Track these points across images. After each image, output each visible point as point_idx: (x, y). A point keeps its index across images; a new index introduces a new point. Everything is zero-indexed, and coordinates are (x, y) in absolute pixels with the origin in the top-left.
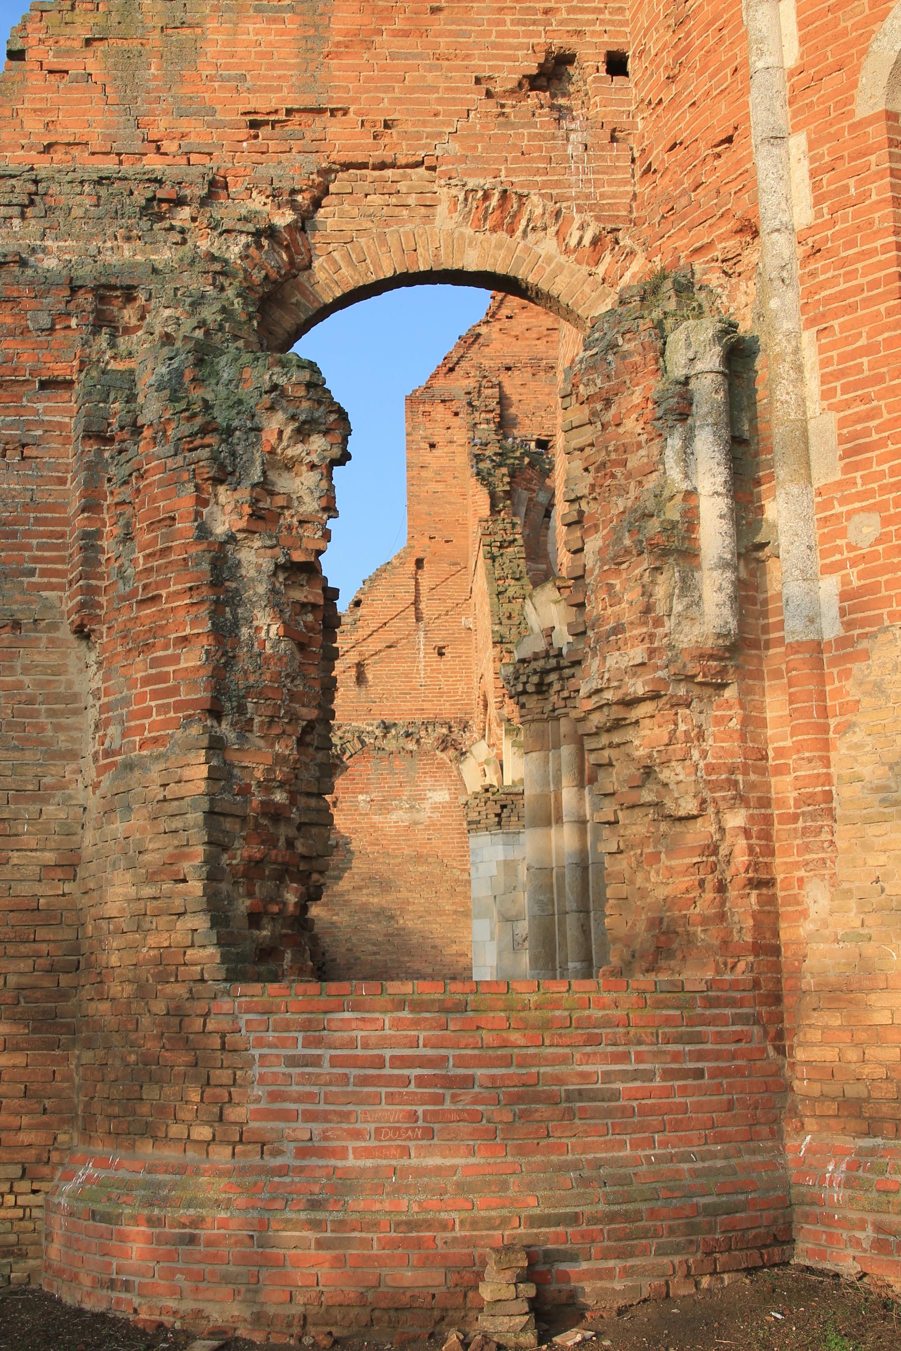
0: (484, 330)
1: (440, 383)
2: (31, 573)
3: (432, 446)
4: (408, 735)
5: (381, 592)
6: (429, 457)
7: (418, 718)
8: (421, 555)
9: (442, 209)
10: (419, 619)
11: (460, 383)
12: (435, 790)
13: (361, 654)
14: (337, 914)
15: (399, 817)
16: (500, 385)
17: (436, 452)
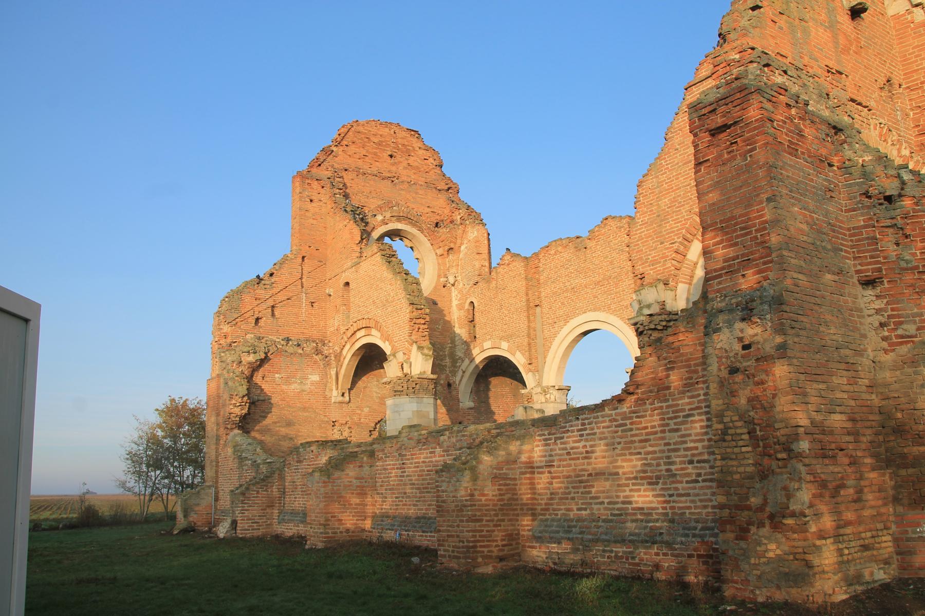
0: (334, 149)
1: (314, 170)
2: (841, 250)
4: (299, 345)
6: (309, 206)
7: (302, 337)
9: (872, 127)
10: (302, 287)
11: (324, 173)
13: (274, 301)
17: (313, 204)
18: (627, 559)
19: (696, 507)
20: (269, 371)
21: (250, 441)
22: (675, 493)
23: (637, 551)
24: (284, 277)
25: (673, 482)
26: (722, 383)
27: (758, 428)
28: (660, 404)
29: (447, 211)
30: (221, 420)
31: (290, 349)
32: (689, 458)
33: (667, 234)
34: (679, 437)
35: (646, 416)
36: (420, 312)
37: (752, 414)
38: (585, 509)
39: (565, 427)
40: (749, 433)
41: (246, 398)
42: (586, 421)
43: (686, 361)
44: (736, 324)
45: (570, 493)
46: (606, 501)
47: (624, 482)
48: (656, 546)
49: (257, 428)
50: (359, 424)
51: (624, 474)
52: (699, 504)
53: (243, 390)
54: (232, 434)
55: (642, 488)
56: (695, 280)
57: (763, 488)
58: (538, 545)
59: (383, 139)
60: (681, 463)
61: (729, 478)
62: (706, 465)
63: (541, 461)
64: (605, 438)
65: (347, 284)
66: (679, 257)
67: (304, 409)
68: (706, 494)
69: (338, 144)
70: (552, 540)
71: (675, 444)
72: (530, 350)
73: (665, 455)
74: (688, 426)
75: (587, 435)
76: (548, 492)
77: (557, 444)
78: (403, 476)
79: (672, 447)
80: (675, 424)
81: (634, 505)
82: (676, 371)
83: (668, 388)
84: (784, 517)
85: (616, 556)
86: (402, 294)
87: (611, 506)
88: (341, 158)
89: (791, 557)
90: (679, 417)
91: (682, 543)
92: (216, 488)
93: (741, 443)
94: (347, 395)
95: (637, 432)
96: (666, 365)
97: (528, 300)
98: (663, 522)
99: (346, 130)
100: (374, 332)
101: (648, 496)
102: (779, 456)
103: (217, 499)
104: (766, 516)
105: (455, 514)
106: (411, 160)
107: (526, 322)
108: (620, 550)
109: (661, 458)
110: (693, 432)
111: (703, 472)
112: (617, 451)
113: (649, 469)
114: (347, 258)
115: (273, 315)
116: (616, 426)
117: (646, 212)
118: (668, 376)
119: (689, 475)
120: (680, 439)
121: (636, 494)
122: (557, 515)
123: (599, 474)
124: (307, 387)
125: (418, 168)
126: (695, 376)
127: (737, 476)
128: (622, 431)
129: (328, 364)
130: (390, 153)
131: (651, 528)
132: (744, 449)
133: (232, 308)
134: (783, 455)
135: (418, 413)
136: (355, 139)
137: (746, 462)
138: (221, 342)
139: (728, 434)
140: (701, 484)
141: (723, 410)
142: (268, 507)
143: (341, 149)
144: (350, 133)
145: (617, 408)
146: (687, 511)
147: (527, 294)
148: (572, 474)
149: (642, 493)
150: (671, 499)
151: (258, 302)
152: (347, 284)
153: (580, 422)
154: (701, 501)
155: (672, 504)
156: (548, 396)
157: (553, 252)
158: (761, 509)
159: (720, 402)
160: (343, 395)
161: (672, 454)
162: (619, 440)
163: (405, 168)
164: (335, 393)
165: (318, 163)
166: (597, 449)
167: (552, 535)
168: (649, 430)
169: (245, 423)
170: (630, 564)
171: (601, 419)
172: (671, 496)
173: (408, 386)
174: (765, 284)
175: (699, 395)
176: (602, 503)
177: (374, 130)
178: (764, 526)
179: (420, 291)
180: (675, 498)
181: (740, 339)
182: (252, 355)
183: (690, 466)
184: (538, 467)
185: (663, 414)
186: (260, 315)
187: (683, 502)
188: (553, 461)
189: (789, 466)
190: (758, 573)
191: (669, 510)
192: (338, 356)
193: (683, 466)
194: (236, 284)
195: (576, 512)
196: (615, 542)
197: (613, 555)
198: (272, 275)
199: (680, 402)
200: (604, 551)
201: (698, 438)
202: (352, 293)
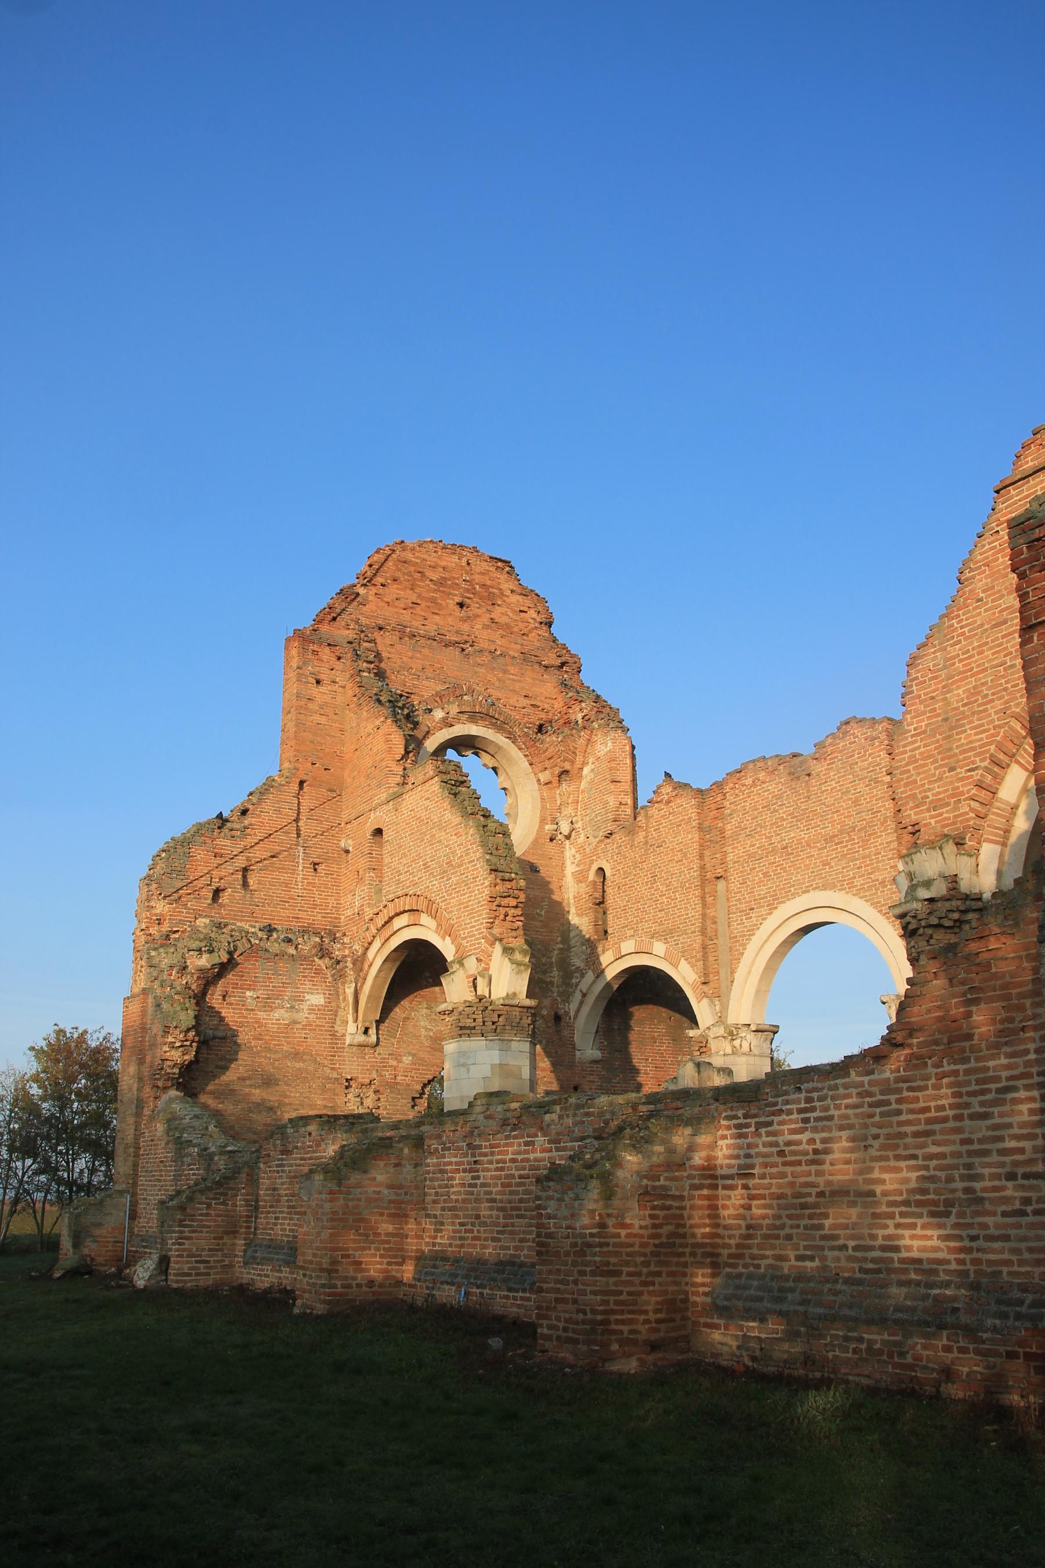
0: (362, 591)
1: (325, 628)
3: (318, 682)
4: (290, 941)
5: (268, 805)
6: (314, 691)
7: (295, 925)
8: (305, 778)
10: (299, 835)
11: (342, 633)
12: (312, 994)
13: (248, 859)
14: (223, 1103)
15: (281, 1014)
16: (373, 641)
17: (322, 689)
18: (891, 1355)
19: (1021, 1263)
20: (235, 986)
21: (197, 1110)
22: (982, 1233)
23: (910, 1342)
24: (268, 817)
25: (977, 1213)
28: (953, 1067)
29: (558, 705)
30: (146, 1071)
31: (274, 947)
32: (1008, 1169)
33: (962, 752)
34: (988, 1128)
35: (926, 1088)
36: (508, 885)
38: (812, 1258)
39: (776, 1104)
41: (192, 1034)
42: (815, 1095)
43: (1003, 987)
45: (782, 1227)
46: (851, 1243)
47: (884, 1209)
48: (945, 1333)
49: (210, 1088)
50: (393, 1085)
51: (885, 1194)
52: (1026, 1256)
53: (187, 1018)
54: (165, 1097)
56: (1013, 838)
58: (722, 1322)
59: (447, 575)
63: (729, 1166)
64: (850, 1127)
65: (379, 832)
66: (983, 795)
67: (297, 1056)
69: (368, 581)
70: (749, 1314)
71: (980, 1141)
72: (705, 958)
73: (961, 1161)
74: (1006, 1108)
75: (816, 1119)
76: (743, 1223)
77: (759, 1135)
78: (475, 1185)
79: (976, 1146)
80: (982, 1104)
81: (904, 1254)
82: (983, 1006)
83: (969, 1037)
85: (869, 1349)
86: (477, 853)
87: (859, 1254)
88: (373, 607)
90: (989, 1091)
91: (995, 1329)
92: (134, 1195)
94: (372, 1031)
95: (911, 1117)
96: (964, 994)
97: (702, 868)
98: (958, 1287)
99: (382, 557)
100: (425, 919)
101: (930, 1238)
103: (133, 1216)
105: (570, 1260)
106: (497, 613)
107: (699, 908)
108: (878, 1337)
110: (1016, 1119)
113: (932, 1186)
114: (379, 786)
115: (245, 884)
116: (870, 1105)
117: (924, 713)
118: (968, 1015)
119: (1006, 1200)
120: (991, 1133)
121: (907, 1233)
122: (758, 1266)
123: (839, 1194)
124: (301, 1016)
125: (507, 627)
126: (1019, 1016)
128: (882, 1114)
129: (340, 976)
130: (458, 599)
131: (935, 1296)
133: (171, 868)
135: (502, 1069)
136: (398, 574)
138: (152, 931)
140: (1030, 1219)
142: (228, 1233)
143: (373, 590)
144: (390, 563)
145: (872, 1072)
146: (1005, 1270)
147: (701, 857)
148: (788, 1191)
149: (918, 1231)
150: (973, 1244)
151: (219, 861)
152: (379, 832)
153: (803, 1096)
154: (1031, 1250)
155: (975, 1255)
156: (737, 1043)
157: (749, 781)
160: (366, 1031)
161: (977, 1160)
162: (875, 1131)
163: (485, 627)
164: (351, 1028)
165: (331, 615)
166: (836, 1146)
167: (749, 1304)
168: (933, 1114)
169: (190, 1079)
170: (896, 1366)
171: (841, 1091)
172: (973, 1238)
173: (484, 1019)
175: (1027, 1052)
176: (844, 1247)
177: (432, 559)
179: (509, 847)
180: (981, 1243)
182: (205, 956)
185: (958, 1084)
186: (222, 884)
187: (997, 1253)
188: (752, 1166)
191: (969, 1266)
192: (360, 962)
193: (997, 1183)
194: (180, 827)
195: (793, 1262)
196: (870, 1322)
197: (864, 1346)
198: (244, 812)
199: (991, 1064)
200: (847, 1339)
201: (1024, 1131)
202: (387, 848)
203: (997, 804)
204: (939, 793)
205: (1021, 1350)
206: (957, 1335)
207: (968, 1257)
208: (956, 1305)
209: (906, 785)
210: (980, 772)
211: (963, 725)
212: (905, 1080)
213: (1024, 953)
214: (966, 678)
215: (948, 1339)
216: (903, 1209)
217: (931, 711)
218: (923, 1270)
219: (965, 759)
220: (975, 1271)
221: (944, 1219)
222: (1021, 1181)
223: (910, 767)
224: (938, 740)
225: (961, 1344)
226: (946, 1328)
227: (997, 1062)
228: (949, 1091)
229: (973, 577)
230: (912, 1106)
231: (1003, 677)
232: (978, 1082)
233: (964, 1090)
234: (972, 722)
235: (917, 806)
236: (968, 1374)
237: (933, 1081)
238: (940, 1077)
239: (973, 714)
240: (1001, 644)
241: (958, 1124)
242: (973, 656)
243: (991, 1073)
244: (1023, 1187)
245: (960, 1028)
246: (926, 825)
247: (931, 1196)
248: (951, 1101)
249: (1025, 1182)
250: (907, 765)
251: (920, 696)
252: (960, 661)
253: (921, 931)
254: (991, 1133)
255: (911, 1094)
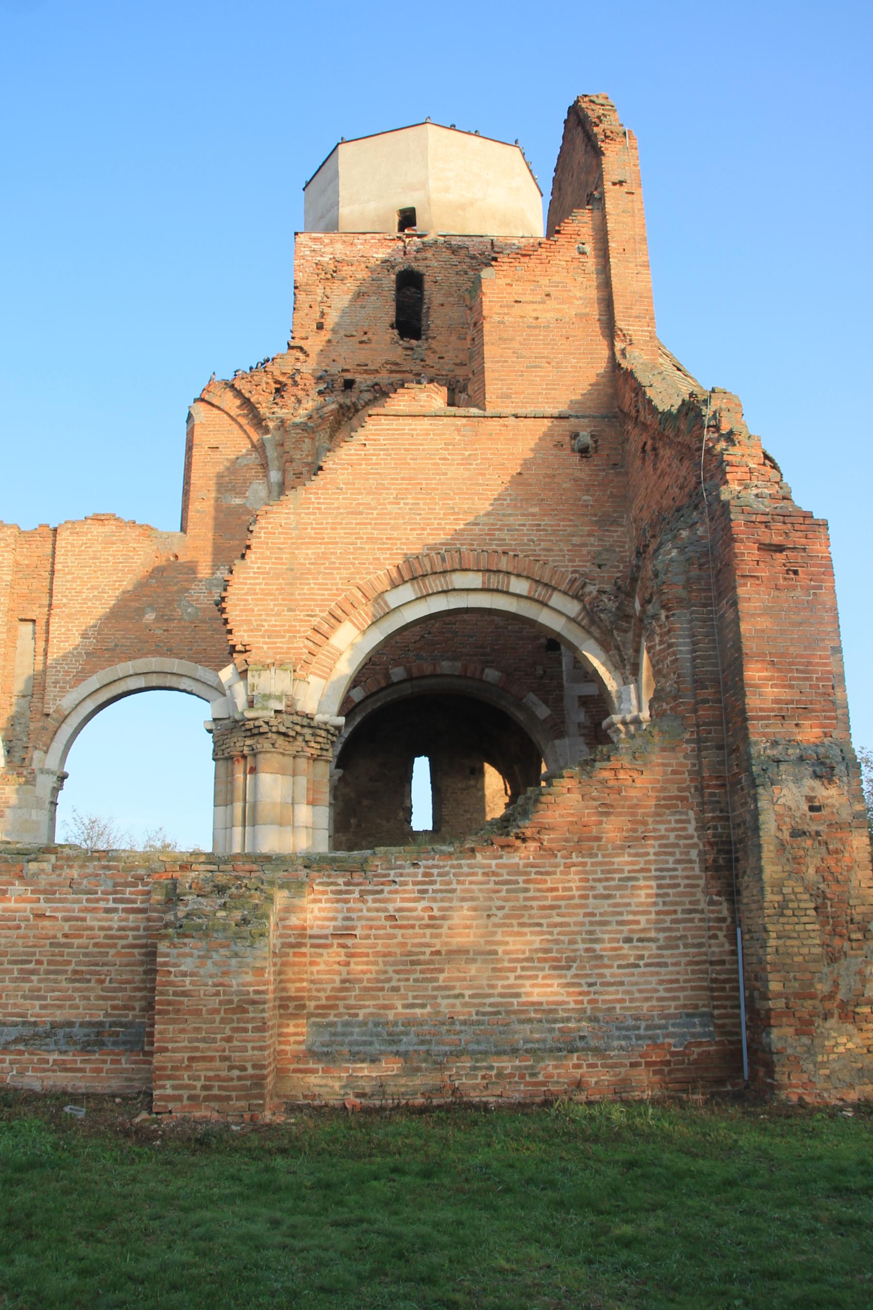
18: (522, 1077)
19: (632, 1000)
22: (599, 981)
23: (542, 1064)
25: (597, 967)
26: (782, 846)
27: (829, 903)
28: (580, 859)
32: (625, 935)
33: (302, 600)
34: (609, 905)
35: (554, 873)
37: (822, 886)
38: (423, 1006)
40: (816, 909)
42: (435, 871)
43: (629, 807)
44: (805, 780)
45: (389, 980)
46: (467, 993)
47: (506, 964)
48: (575, 1055)
51: (506, 952)
52: (637, 995)
55: (541, 974)
56: (334, 677)
57: (832, 973)
58: (320, 1066)
60: (611, 940)
61: (788, 961)
62: (653, 945)
63: (322, 927)
64: (472, 899)
66: (318, 638)
68: (647, 982)
70: (356, 1057)
71: (601, 914)
73: (584, 929)
74: (628, 892)
76: (337, 978)
77: (364, 901)
79: (598, 918)
80: (605, 888)
81: (524, 999)
82: (612, 818)
83: (598, 839)
84: (857, 1005)
85: (500, 1075)
87: (476, 1001)
89: (865, 1050)
90: (613, 879)
91: (621, 1048)
93: (805, 919)
95: (538, 894)
96: (596, 808)
98: (579, 1021)
101: (551, 986)
102: (854, 936)
104: (835, 1004)
105: (218, 1018)
108: (508, 1064)
109: (579, 933)
110: (636, 900)
111: (646, 953)
112: (494, 920)
113: (555, 947)
116: (496, 883)
117: (269, 558)
118: (601, 823)
119: (625, 957)
120: (611, 909)
121: (528, 982)
122: (357, 1015)
123: (456, 953)
126: (641, 828)
127: (799, 959)
128: (508, 891)
131: (560, 1029)
132: (809, 927)
134: (859, 936)
137: (810, 942)
139: (788, 908)
140: (642, 969)
141: (783, 879)
145: (501, 857)
146: (618, 1006)
148: (398, 951)
149: (540, 981)
150: (592, 989)
154: (640, 991)
155: (592, 996)
158: (831, 996)
159: (779, 868)
162: (500, 903)
166: (455, 914)
167: (356, 1049)
168: (560, 893)
170: (527, 1084)
171: (465, 870)
172: (590, 985)
174: (826, 741)
175: (648, 854)
176: (461, 995)
178: (832, 1017)
180: (597, 988)
181: (810, 799)
183: (626, 946)
184: (312, 937)
185: (586, 872)
187: (612, 994)
189: (865, 947)
190: (827, 1072)
191: (586, 1005)
193: (615, 945)
195: (400, 1010)
196: (499, 1053)
197: (494, 1072)
199: (616, 860)
200: (475, 1068)
201: (641, 909)
203: (328, 648)
204: (275, 626)
205: (643, 1061)
206: (587, 1055)
207: (586, 999)
208: (581, 1034)
209: (242, 611)
210: (318, 619)
211: (308, 579)
212: (533, 866)
213: (650, 786)
214: (316, 543)
215: (578, 1059)
216: (526, 964)
217: (276, 558)
218: (544, 1010)
219: (305, 605)
220: (592, 1009)
221: (564, 972)
222: (635, 943)
223: (249, 598)
224: (280, 584)
225: (591, 1061)
226: (577, 1051)
227: (620, 859)
228: (577, 877)
229: (336, 469)
230: (539, 886)
231: (352, 553)
232: (603, 872)
233: (591, 877)
234: (317, 579)
235: (252, 631)
236: (596, 1083)
237: (562, 868)
238: (568, 866)
239: (320, 573)
240: (354, 529)
241: (583, 901)
242: (326, 529)
243: (616, 867)
244: (637, 948)
245: (591, 832)
246: (258, 648)
247: (554, 955)
248: (579, 884)
249: (640, 944)
250: (246, 594)
251: (267, 543)
252: (312, 529)
253: (270, 735)
254: (611, 909)
255: (539, 877)
